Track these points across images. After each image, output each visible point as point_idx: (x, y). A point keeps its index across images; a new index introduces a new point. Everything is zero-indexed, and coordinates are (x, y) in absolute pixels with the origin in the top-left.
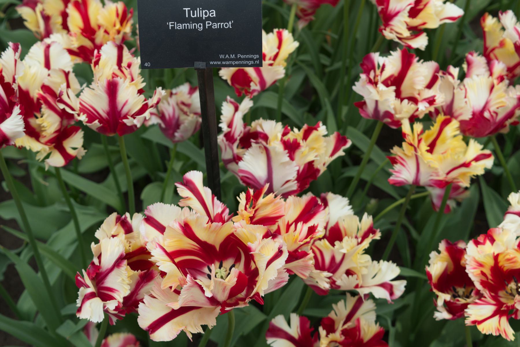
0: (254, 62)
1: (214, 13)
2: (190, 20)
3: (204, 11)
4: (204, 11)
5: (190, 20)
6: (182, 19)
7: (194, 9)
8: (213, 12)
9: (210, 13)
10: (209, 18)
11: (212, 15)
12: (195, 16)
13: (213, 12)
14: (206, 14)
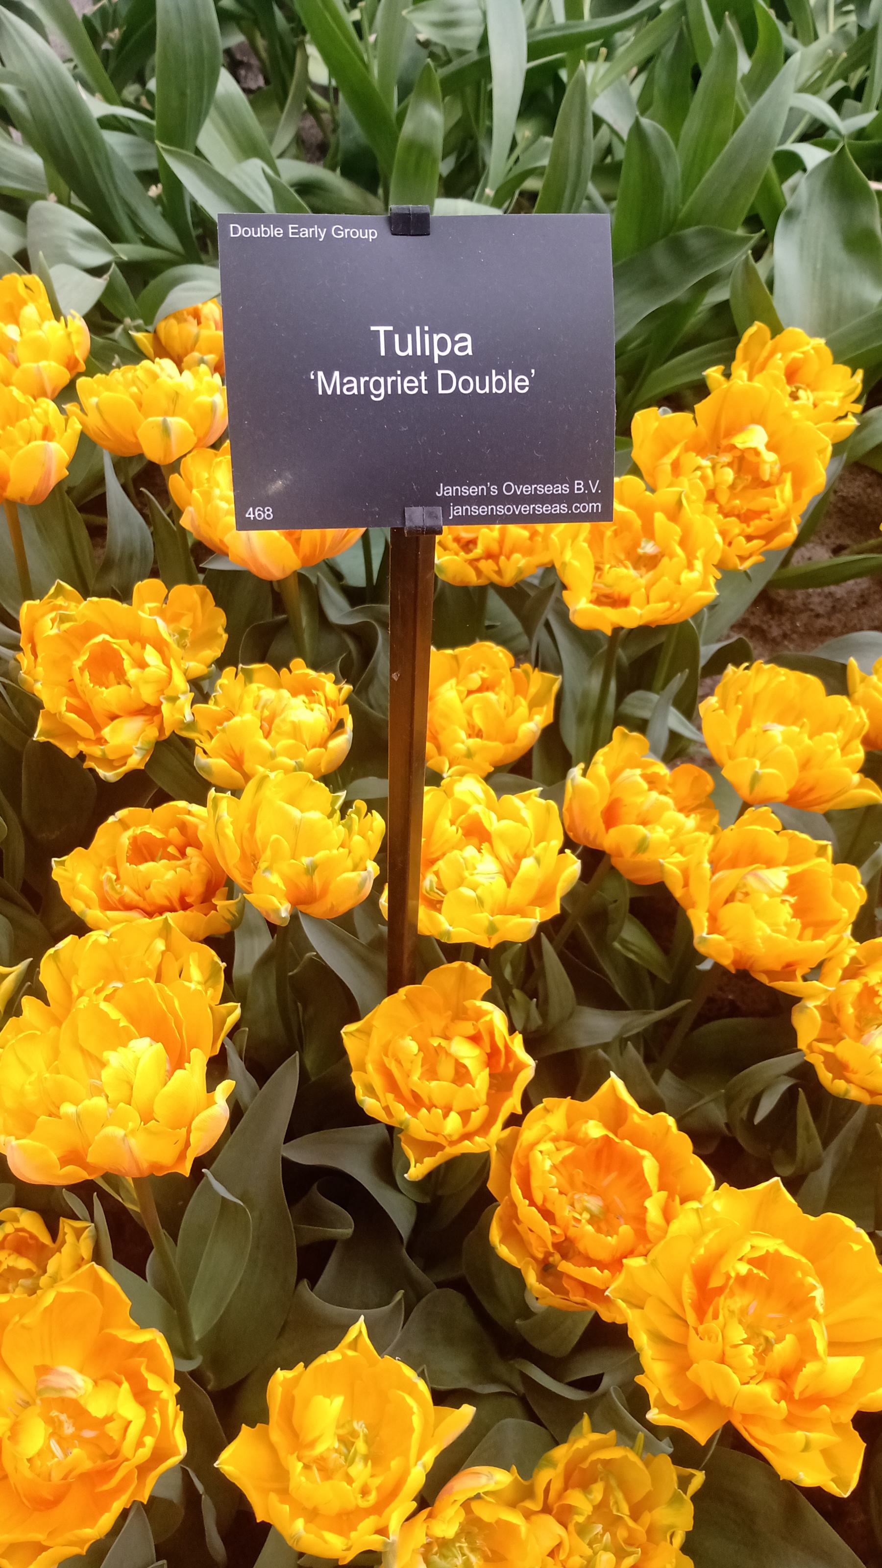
0: (570, 508)
1: (469, 343)
2: (391, 365)
3: (436, 338)
4: (436, 338)
5: (391, 365)
6: (363, 360)
7: (404, 329)
8: (465, 339)
9: (454, 343)
10: (450, 361)
11: (463, 349)
12: (409, 351)
13: (465, 339)
14: (442, 345)
